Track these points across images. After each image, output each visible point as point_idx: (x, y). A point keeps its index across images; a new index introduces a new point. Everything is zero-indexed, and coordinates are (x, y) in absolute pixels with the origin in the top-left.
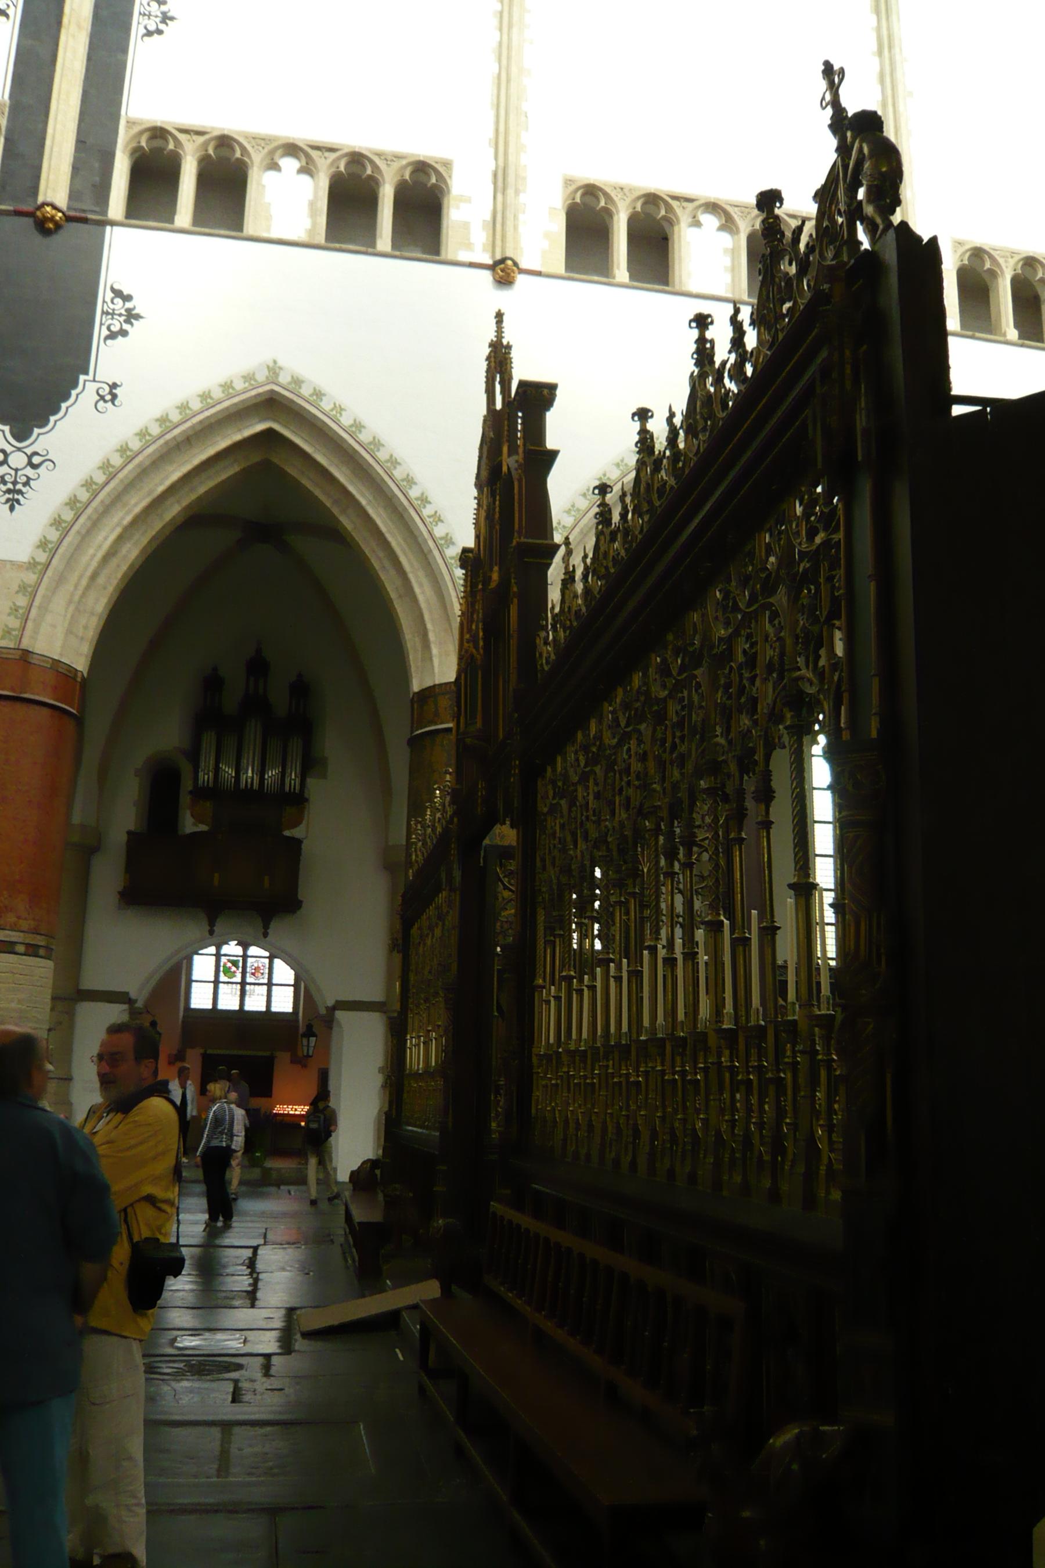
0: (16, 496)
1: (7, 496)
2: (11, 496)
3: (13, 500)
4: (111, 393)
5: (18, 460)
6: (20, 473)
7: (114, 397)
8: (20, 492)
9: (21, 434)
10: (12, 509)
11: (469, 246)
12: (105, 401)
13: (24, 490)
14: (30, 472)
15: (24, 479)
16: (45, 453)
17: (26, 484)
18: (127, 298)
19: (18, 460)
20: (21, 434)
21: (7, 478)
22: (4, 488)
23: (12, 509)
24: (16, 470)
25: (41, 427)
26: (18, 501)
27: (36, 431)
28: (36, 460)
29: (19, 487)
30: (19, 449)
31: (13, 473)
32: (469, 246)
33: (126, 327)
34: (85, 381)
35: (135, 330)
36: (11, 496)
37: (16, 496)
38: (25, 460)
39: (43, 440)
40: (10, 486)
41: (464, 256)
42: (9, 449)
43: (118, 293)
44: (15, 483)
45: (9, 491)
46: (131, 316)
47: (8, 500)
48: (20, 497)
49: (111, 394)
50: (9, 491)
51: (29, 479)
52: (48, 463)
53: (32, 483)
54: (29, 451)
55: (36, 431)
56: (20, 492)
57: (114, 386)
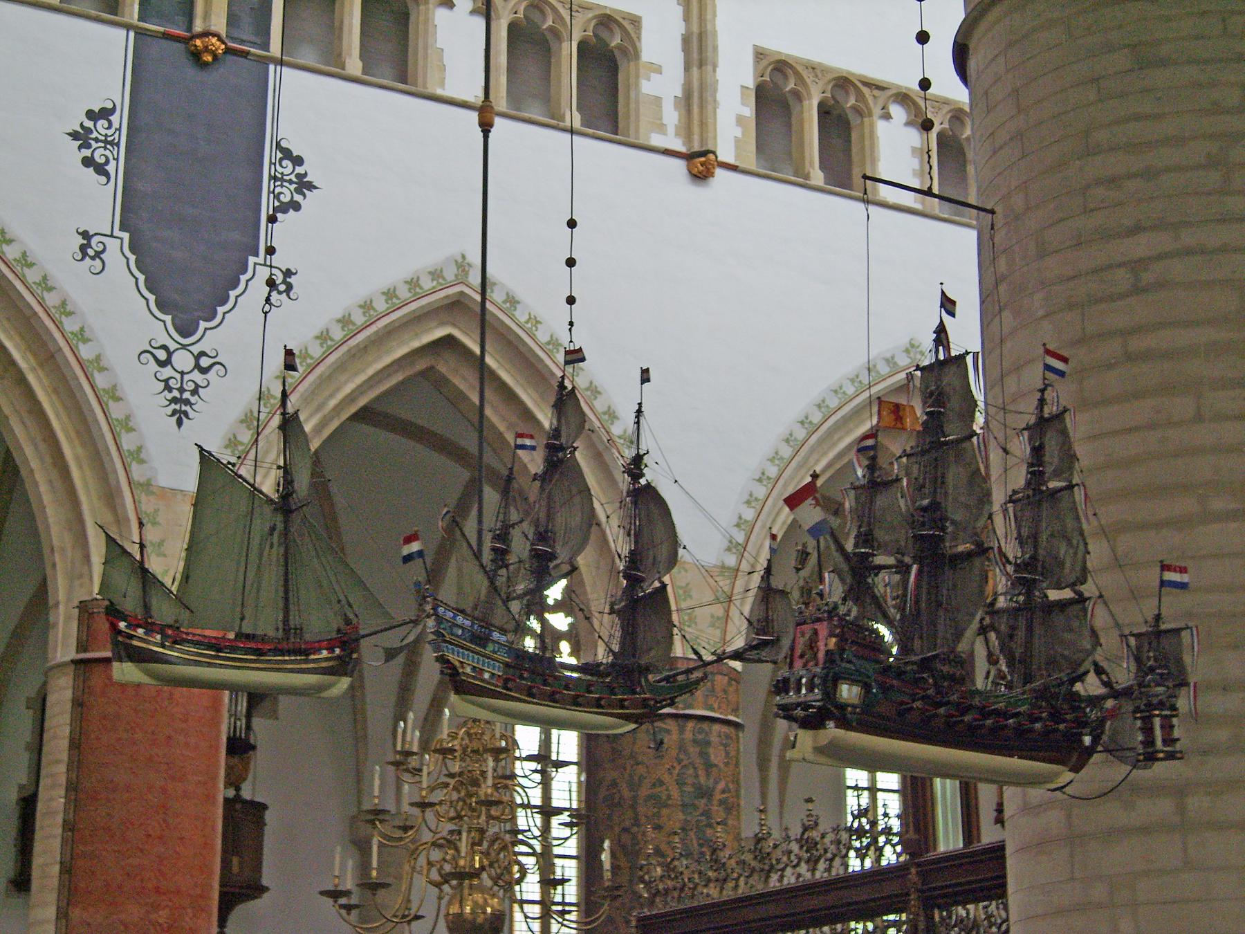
0: (184, 408)
1: (173, 406)
2: (177, 407)
3: (180, 412)
4: (284, 282)
5: (183, 360)
6: (186, 377)
7: (289, 287)
8: (187, 402)
9: (186, 329)
10: (179, 423)
11: (661, 128)
12: (280, 293)
13: (193, 400)
14: (197, 376)
15: (191, 386)
16: (213, 354)
17: (195, 392)
18: (298, 161)
19: (183, 360)
20: (186, 329)
21: (172, 382)
22: (169, 396)
23: (179, 423)
24: (182, 373)
26: (186, 414)
28: (205, 362)
29: (187, 395)
30: (184, 347)
31: (178, 376)
32: (661, 128)
33: (298, 198)
34: (255, 264)
35: (309, 201)
36: (177, 407)
37: (184, 408)
38: (191, 363)
39: (211, 339)
40: (176, 394)
41: (656, 140)
43: (287, 154)
45: (174, 400)
46: (304, 185)
47: (174, 412)
48: (188, 408)
49: (282, 284)
50: (174, 400)
51: (197, 386)
52: (218, 367)
54: (196, 349)
56: (187, 402)
57: (288, 273)
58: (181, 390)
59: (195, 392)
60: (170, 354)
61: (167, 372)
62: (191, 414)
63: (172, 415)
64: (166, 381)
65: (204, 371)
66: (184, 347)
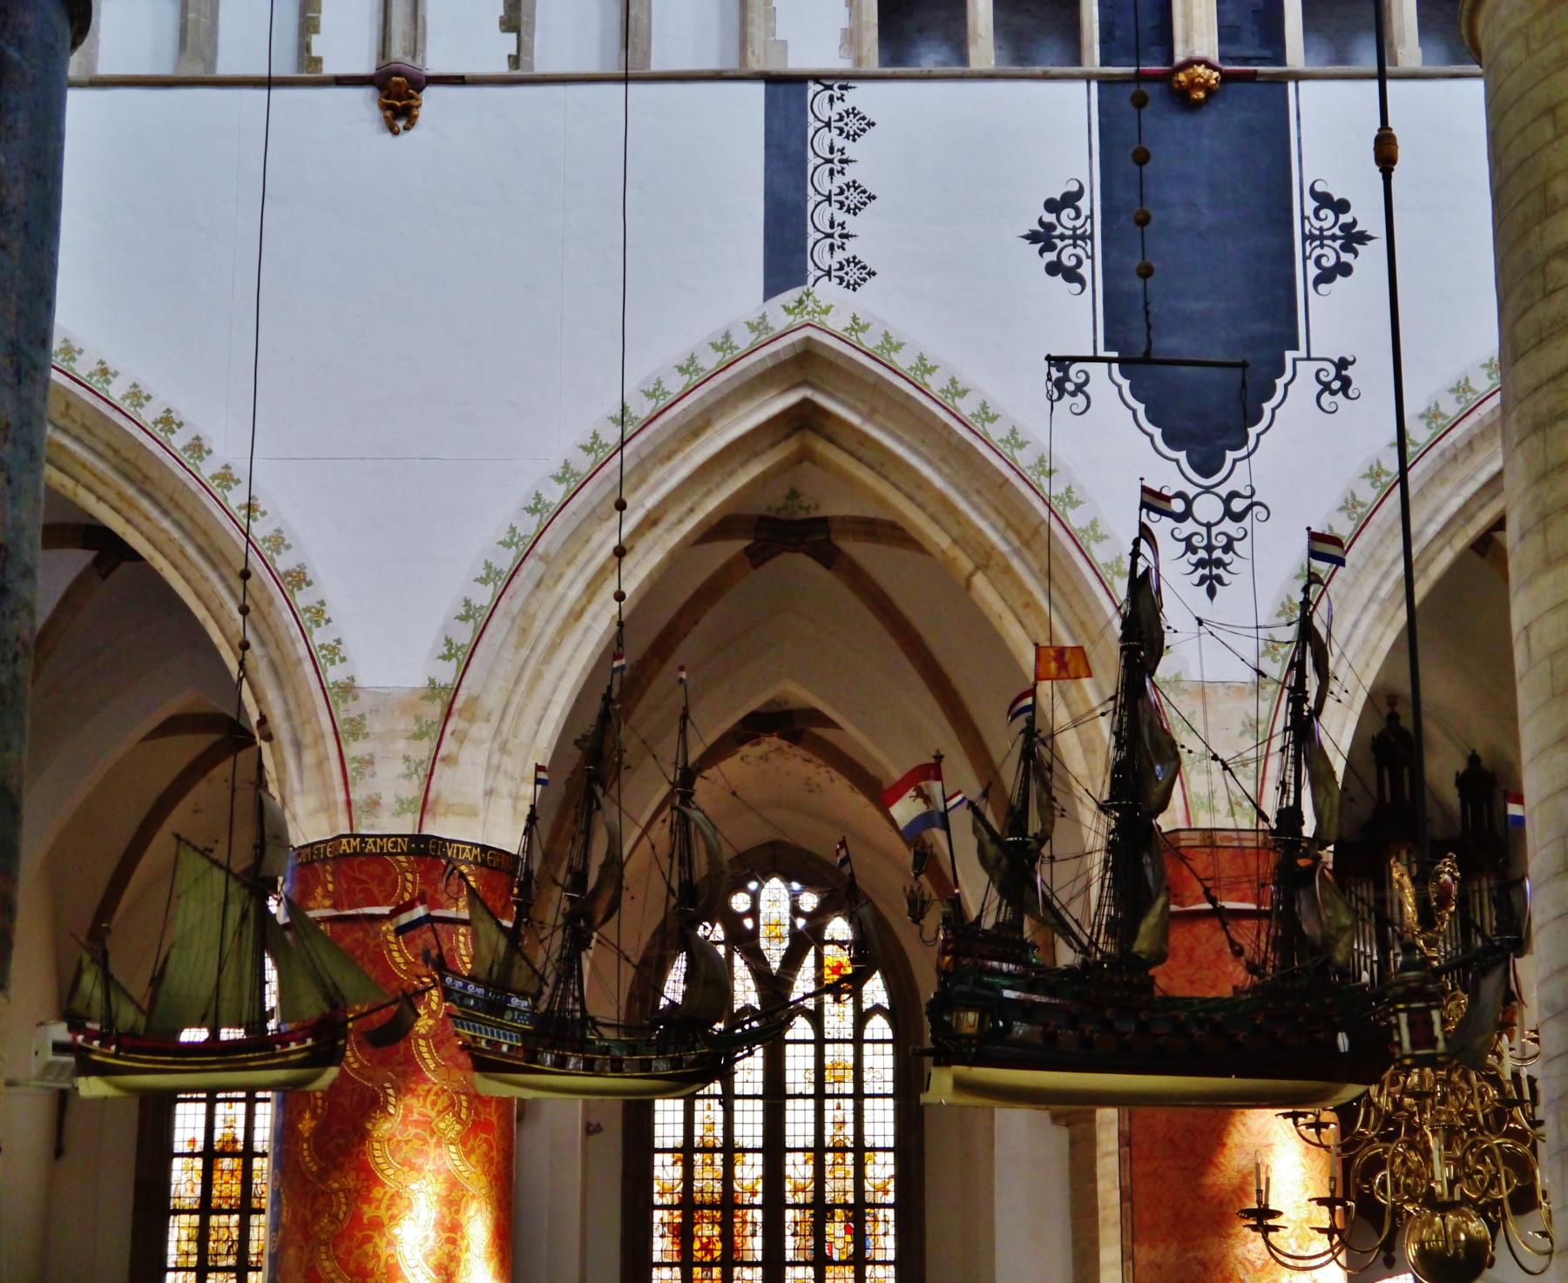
0: (1215, 571)
1: (1201, 571)
2: (1206, 571)
3: (1211, 577)
5: (1210, 508)
6: (1215, 530)
9: (1207, 464)
10: (1211, 593)
13: (1226, 558)
14: (1229, 526)
15: (1223, 540)
17: (1228, 548)
19: (1210, 508)
20: (1207, 464)
21: (1196, 540)
22: (1194, 559)
23: (1211, 593)
24: (1209, 526)
25: (1235, 448)
26: (1219, 579)
27: (1230, 456)
28: (1238, 505)
29: (1217, 554)
30: (1207, 490)
31: (1203, 530)
36: (1206, 571)
37: (1215, 571)
39: (1239, 473)
40: (1203, 554)
42: (1191, 491)
44: (1210, 548)
45: (1201, 564)
47: (1202, 580)
48: (1221, 571)
50: (1201, 564)
51: (1231, 540)
53: (1236, 544)
54: (1223, 491)
55: (1230, 456)
56: (1219, 563)
58: (1210, 548)
59: (1228, 548)
60: (1189, 503)
61: (1188, 527)
62: (1226, 577)
63: (1201, 583)
64: (1188, 540)
65: (1238, 517)
66: (1207, 490)
